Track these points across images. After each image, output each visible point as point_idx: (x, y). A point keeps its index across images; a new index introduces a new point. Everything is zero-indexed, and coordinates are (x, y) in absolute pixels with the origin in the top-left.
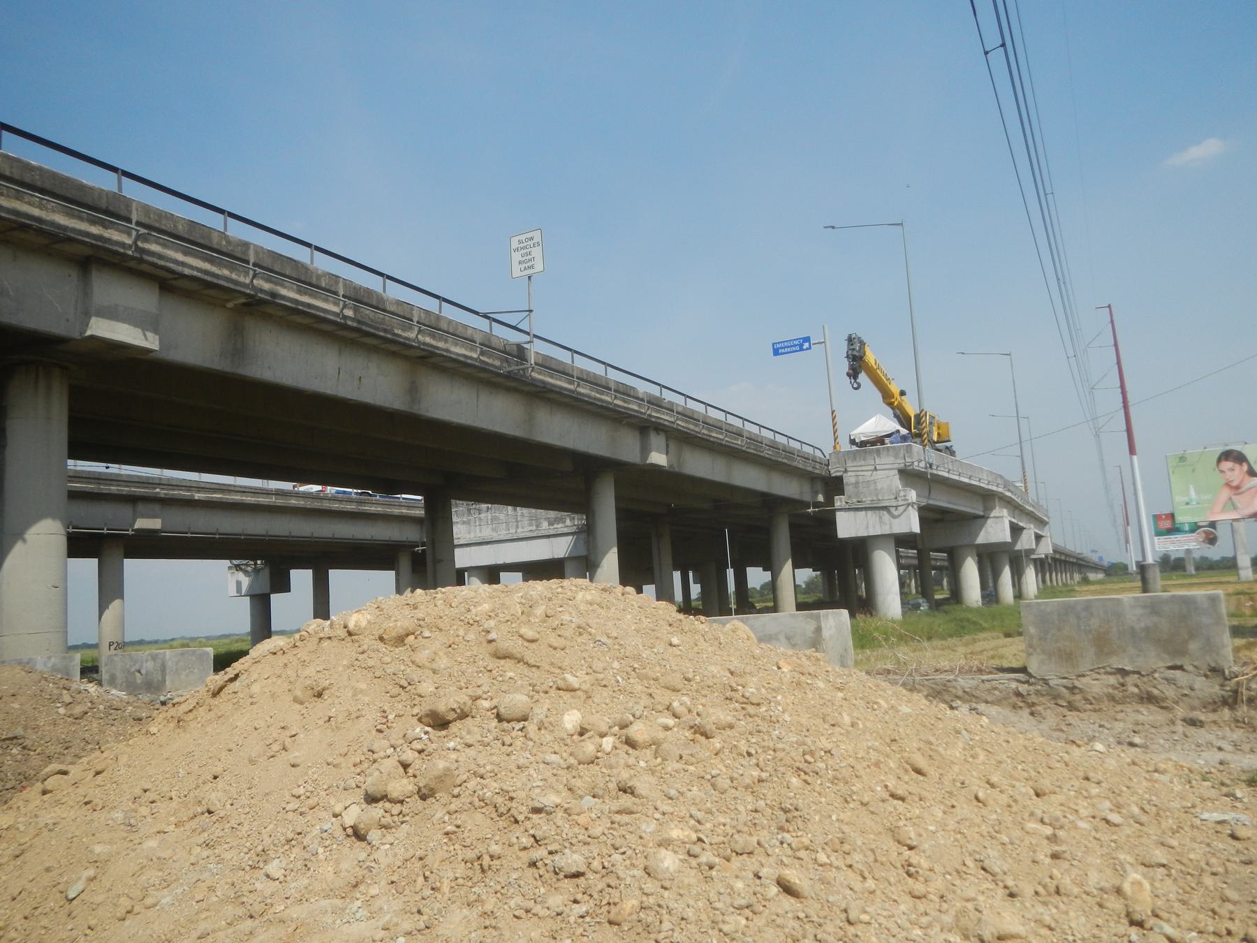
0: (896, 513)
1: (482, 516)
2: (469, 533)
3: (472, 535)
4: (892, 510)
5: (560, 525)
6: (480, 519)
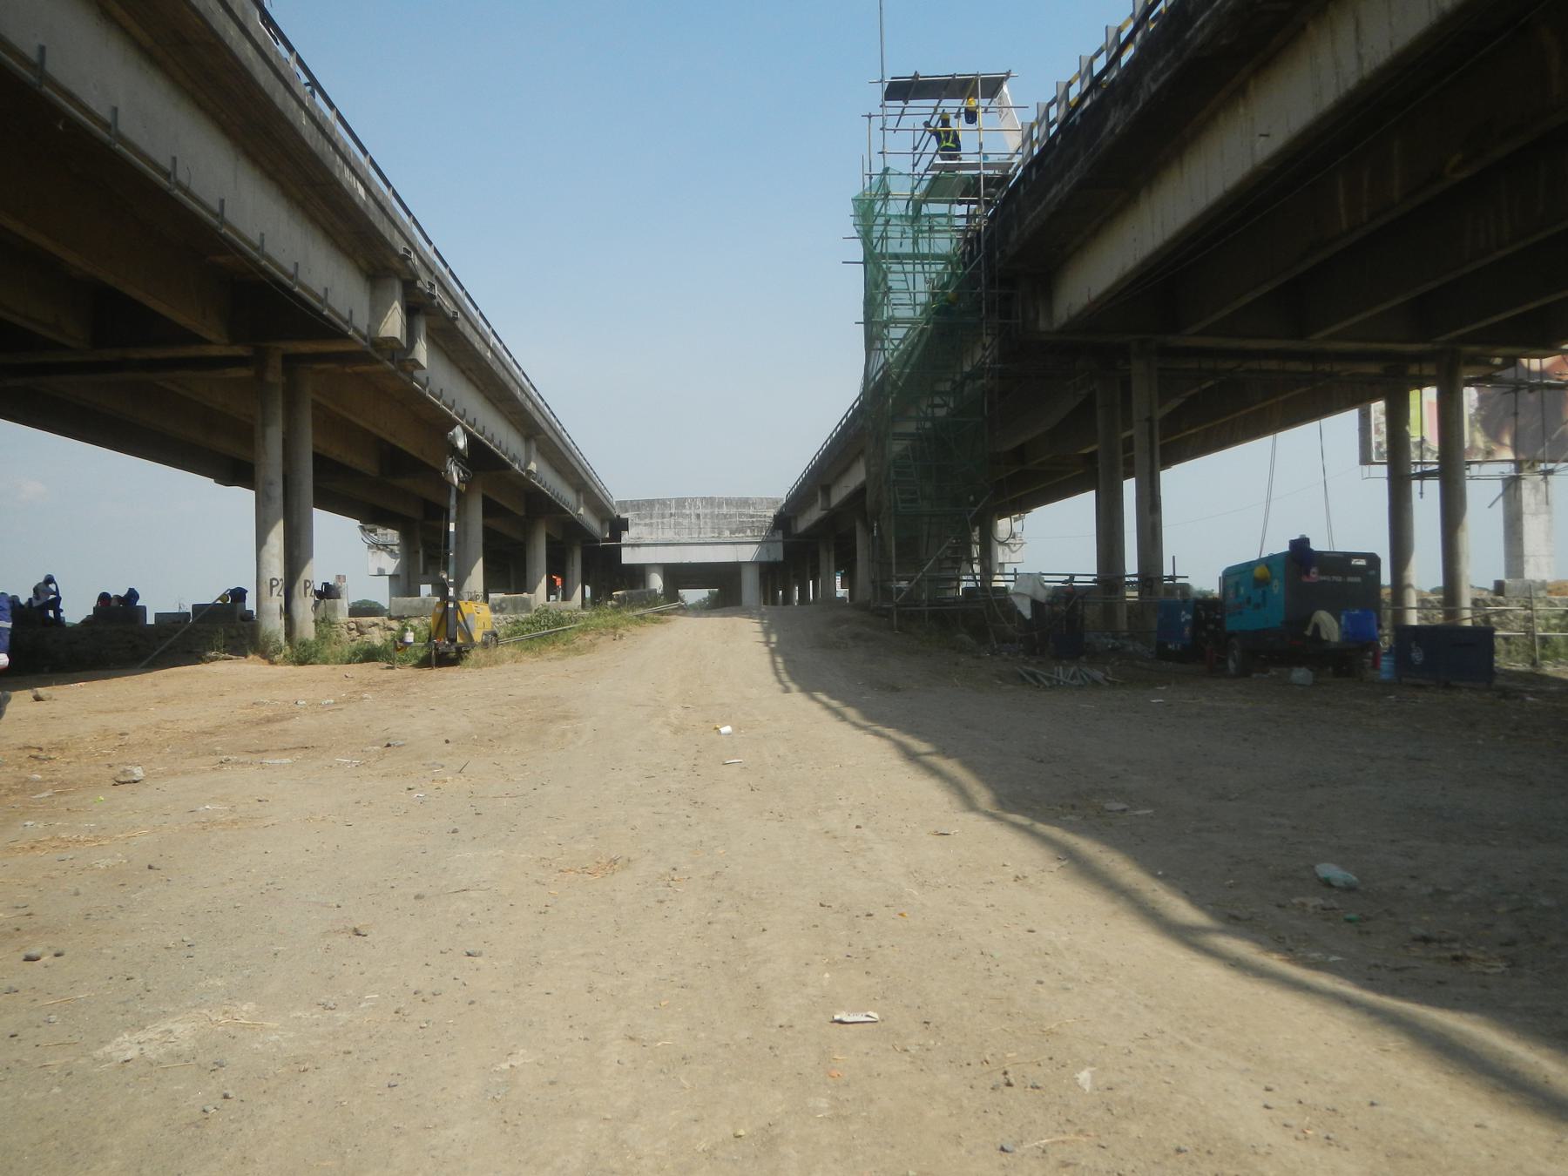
0: (1014, 549)
1: (665, 520)
2: (651, 534)
3: (654, 536)
4: (1012, 546)
5: (741, 535)
6: (663, 523)
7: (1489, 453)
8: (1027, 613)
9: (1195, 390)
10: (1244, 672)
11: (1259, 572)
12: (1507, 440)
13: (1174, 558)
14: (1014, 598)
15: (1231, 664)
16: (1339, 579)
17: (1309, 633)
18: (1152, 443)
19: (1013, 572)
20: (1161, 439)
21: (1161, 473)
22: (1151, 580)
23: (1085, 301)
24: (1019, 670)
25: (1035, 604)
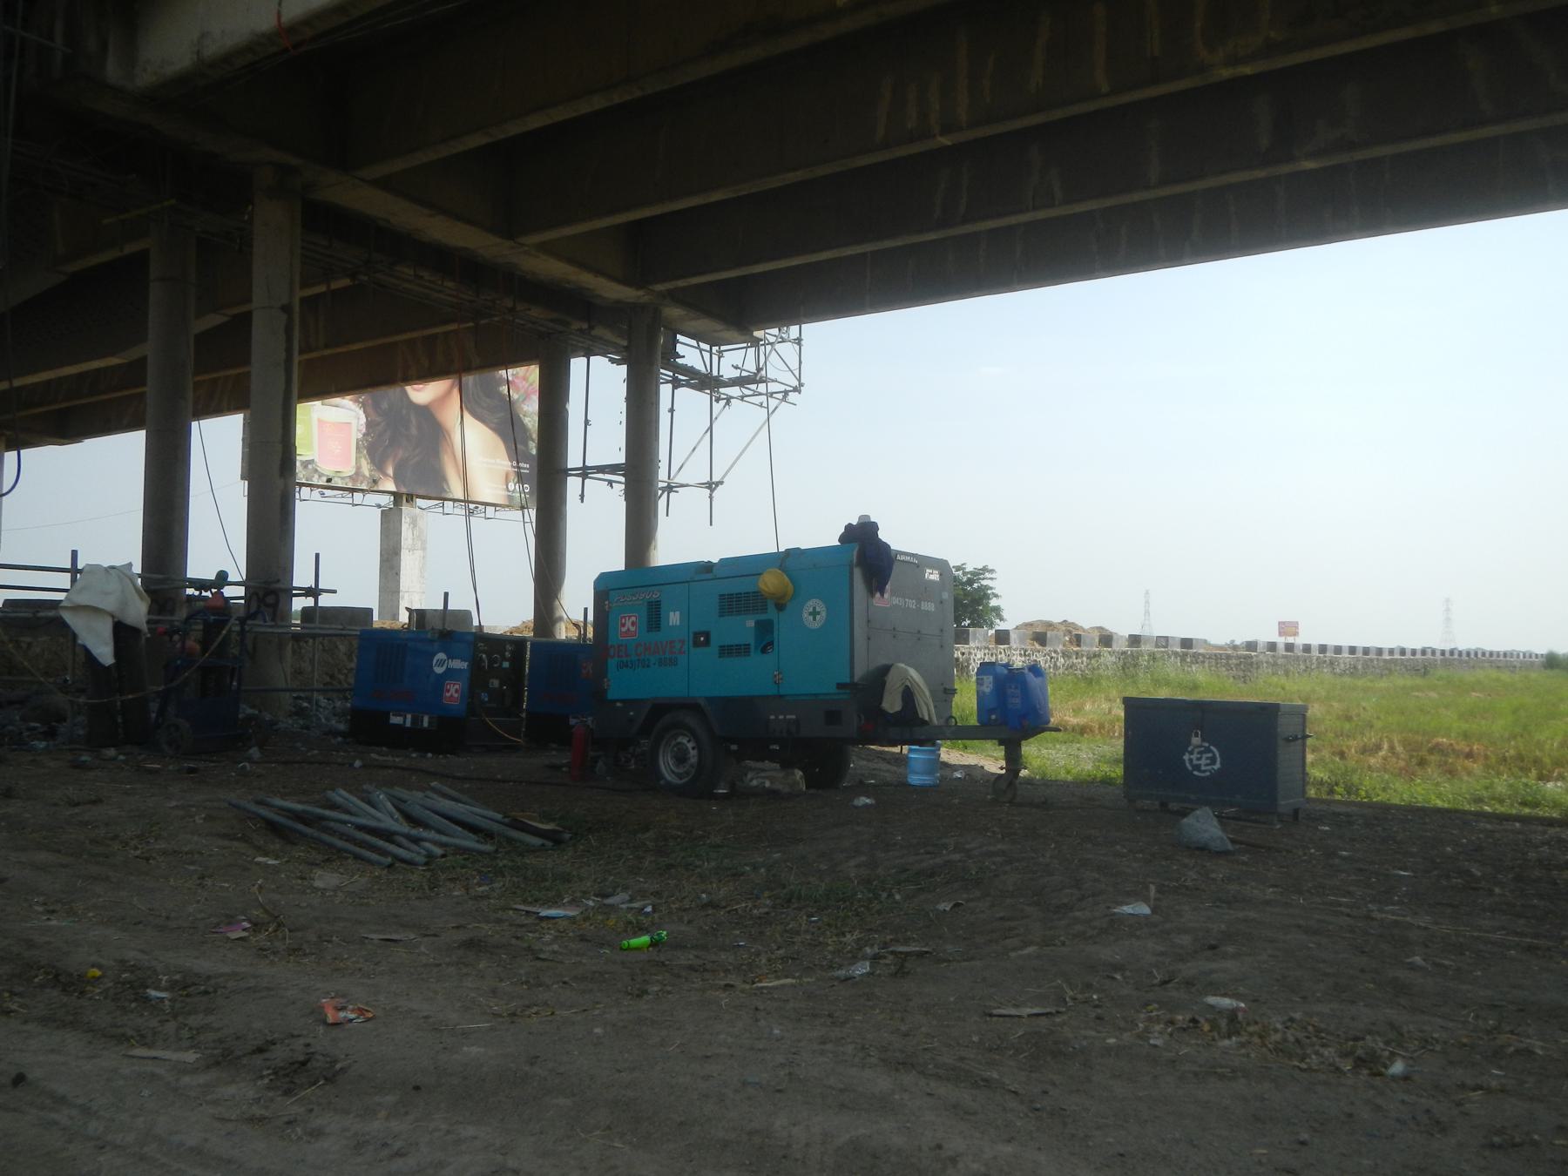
7: (375, 482)
8: (105, 652)
9: (322, 289)
10: (698, 788)
11: (770, 582)
12: (390, 471)
13: (317, 556)
14: (68, 617)
15: (667, 767)
16: (912, 604)
17: (892, 703)
18: (289, 350)
19: (68, 566)
20: (301, 352)
21: (298, 406)
22: (275, 593)
23: (264, 22)
24: (253, 807)
25: (123, 632)
